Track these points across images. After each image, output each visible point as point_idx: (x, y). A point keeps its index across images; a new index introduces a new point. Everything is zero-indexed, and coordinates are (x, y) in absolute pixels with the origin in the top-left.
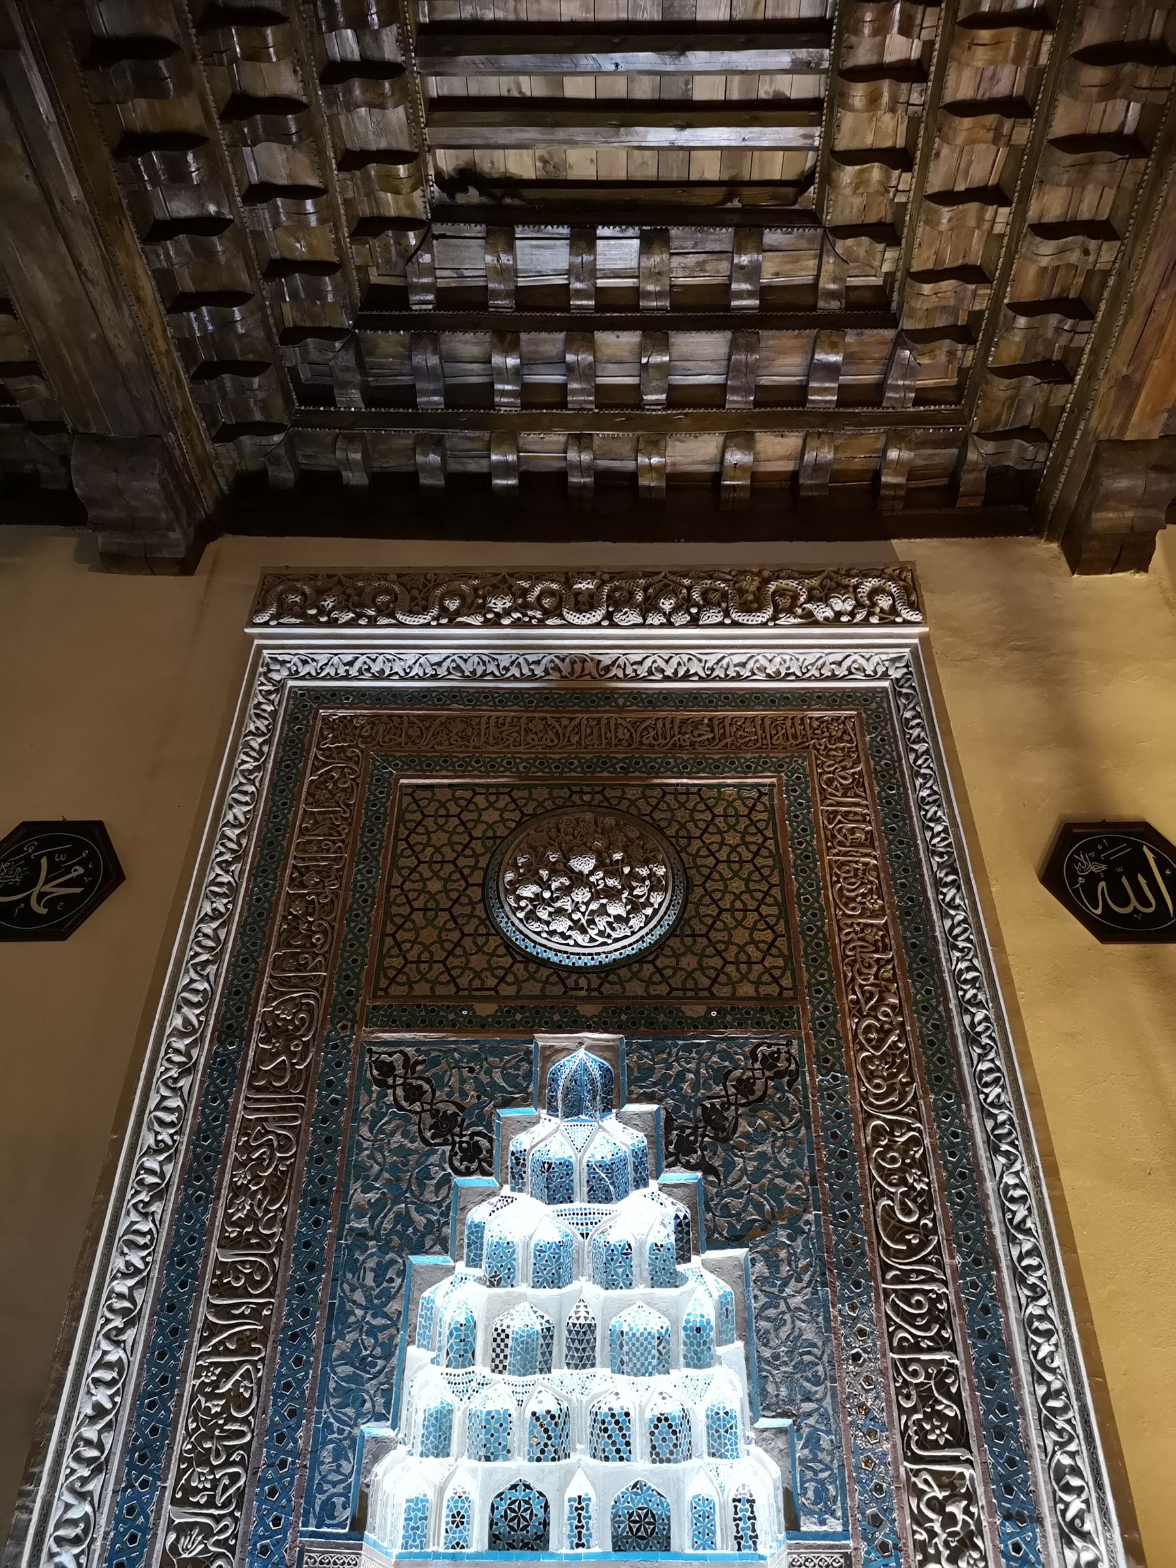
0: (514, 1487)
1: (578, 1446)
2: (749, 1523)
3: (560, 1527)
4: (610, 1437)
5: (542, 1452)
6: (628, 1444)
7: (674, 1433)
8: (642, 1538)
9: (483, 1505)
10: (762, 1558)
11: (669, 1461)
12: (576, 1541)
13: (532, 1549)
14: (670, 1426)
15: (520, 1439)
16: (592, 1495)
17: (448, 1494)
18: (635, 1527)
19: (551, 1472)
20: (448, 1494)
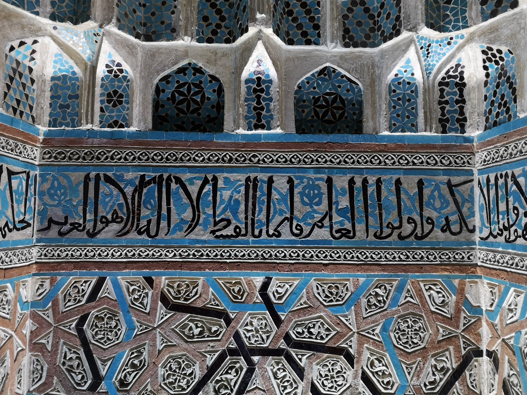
0: (182, 70)
1: (259, 16)
2: (457, 107)
3: (236, 107)
4: (295, 20)
5: (214, 33)
6: (317, 27)
7: (372, 17)
8: (329, 122)
9: (146, 86)
10: (469, 140)
11: (364, 45)
12: (254, 122)
13: (204, 131)
14: (367, 10)
15: (187, 19)
16: (273, 73)
17: (101, 71)
18: (321, 111)
19: (225, 54)
20: (101, 71)
